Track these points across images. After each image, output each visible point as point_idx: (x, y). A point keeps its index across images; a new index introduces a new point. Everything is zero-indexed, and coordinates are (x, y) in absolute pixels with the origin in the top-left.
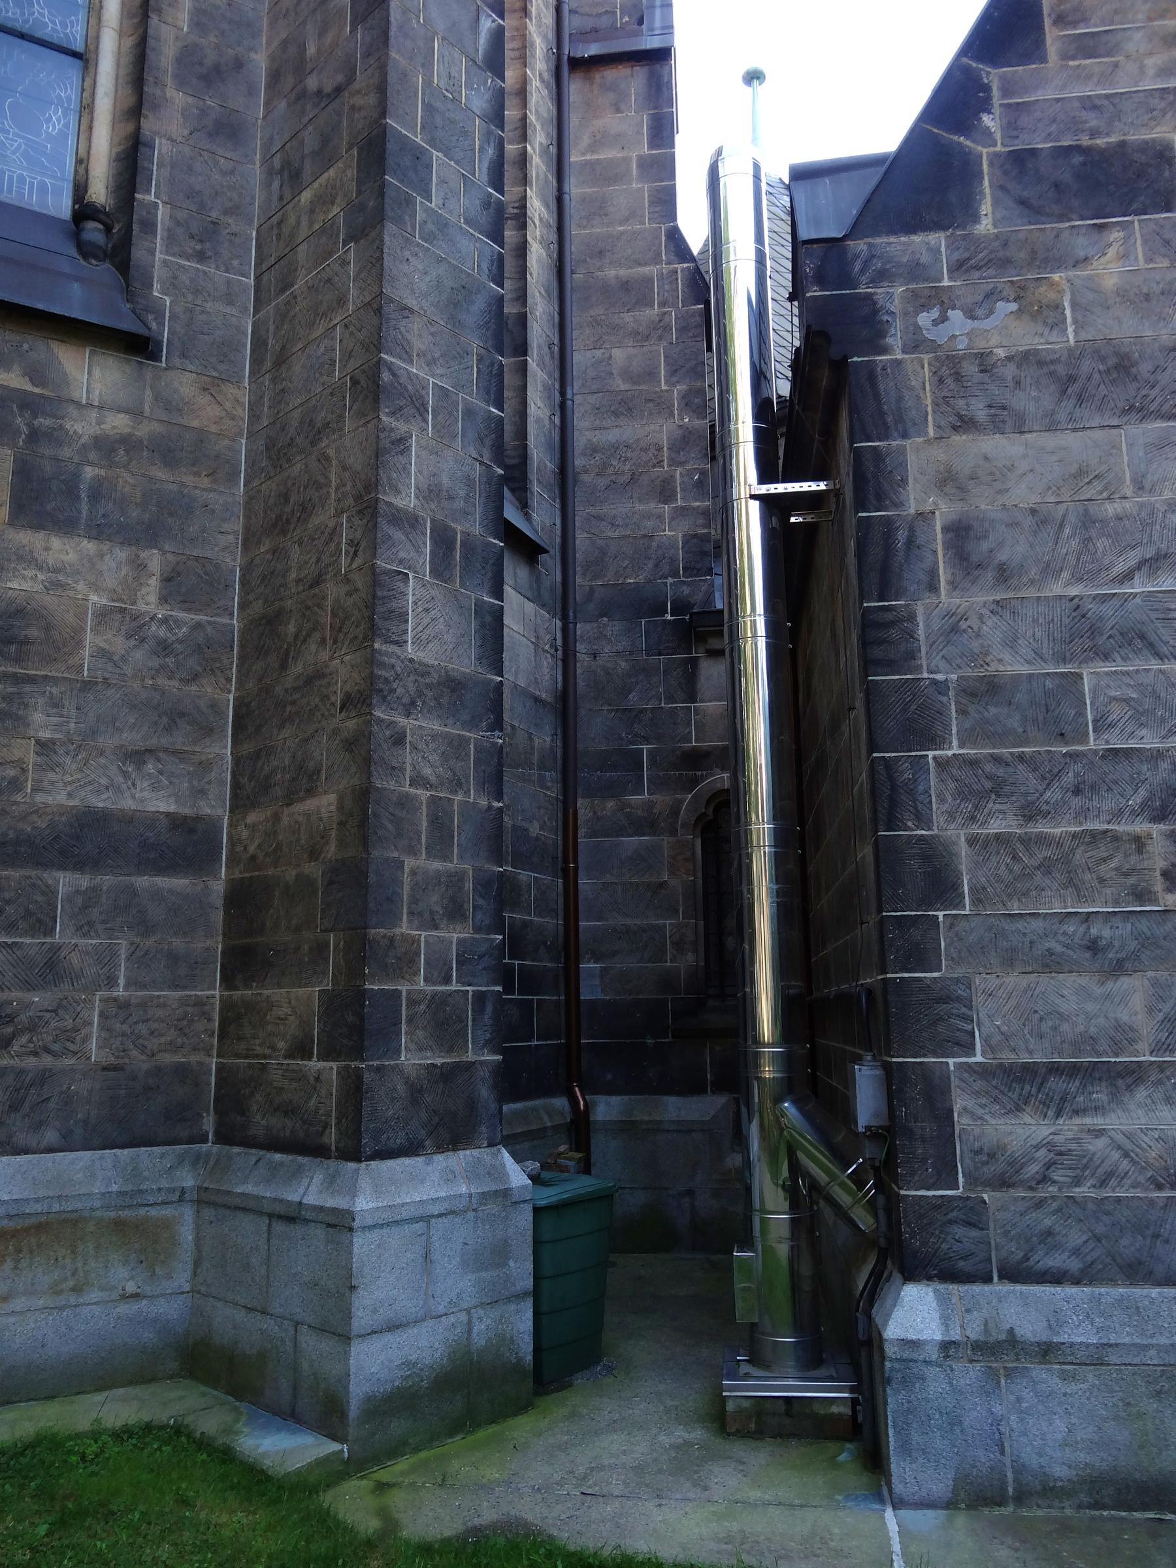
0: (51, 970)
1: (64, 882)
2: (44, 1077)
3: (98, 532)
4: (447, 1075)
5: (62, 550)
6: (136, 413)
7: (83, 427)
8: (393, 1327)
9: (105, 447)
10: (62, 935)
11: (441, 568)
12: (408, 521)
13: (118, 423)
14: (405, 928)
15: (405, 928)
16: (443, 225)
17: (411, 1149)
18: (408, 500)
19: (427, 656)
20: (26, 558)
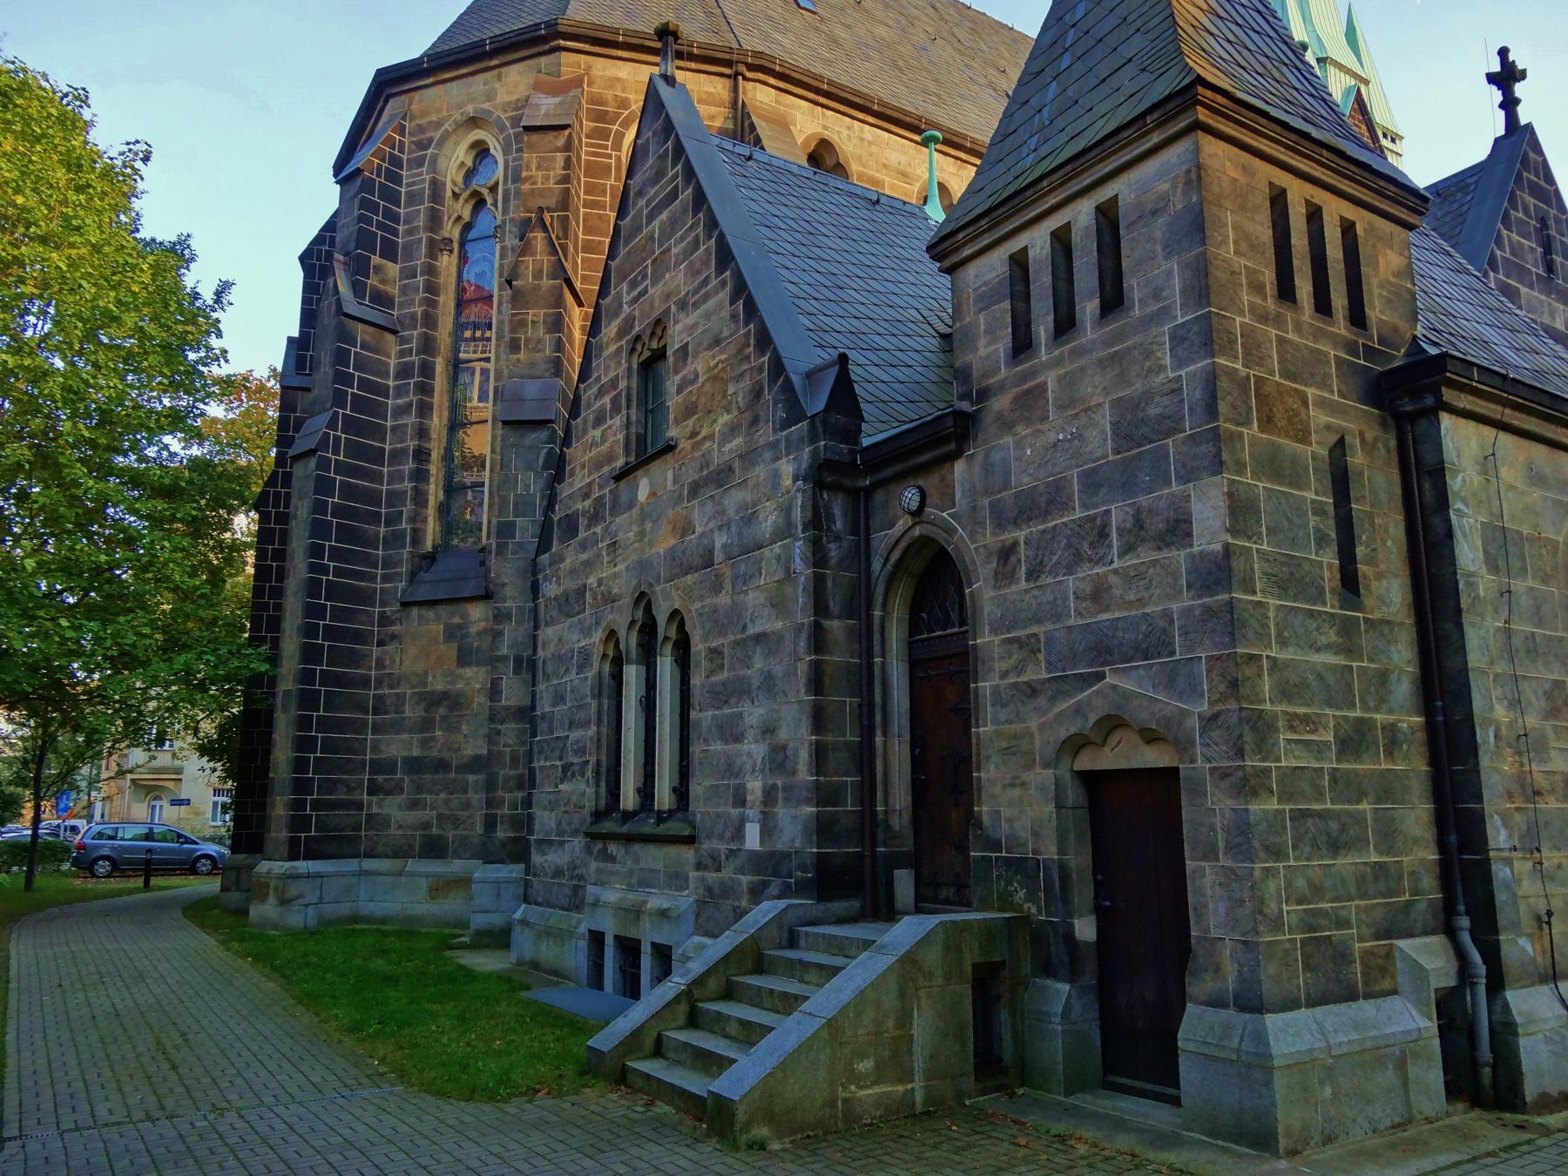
0: (467, 805)
1: (471, 778)
2: (466, 838)
3: (478, 664)
4: (515, 840)
5: (469, 672)
6: (487, 620)
7: (473, 630)
8: (486, 912)
9: (479, 634)
10: (471, 794)
11: (517, 671)
12: (506, 658)
13: (483, 624)
14: (500, 793)
15: (500, 793)
16: (520, 545)
17: (501, 862)
18: (504, 651)
19: (511, 703)
20: (461, 677)
